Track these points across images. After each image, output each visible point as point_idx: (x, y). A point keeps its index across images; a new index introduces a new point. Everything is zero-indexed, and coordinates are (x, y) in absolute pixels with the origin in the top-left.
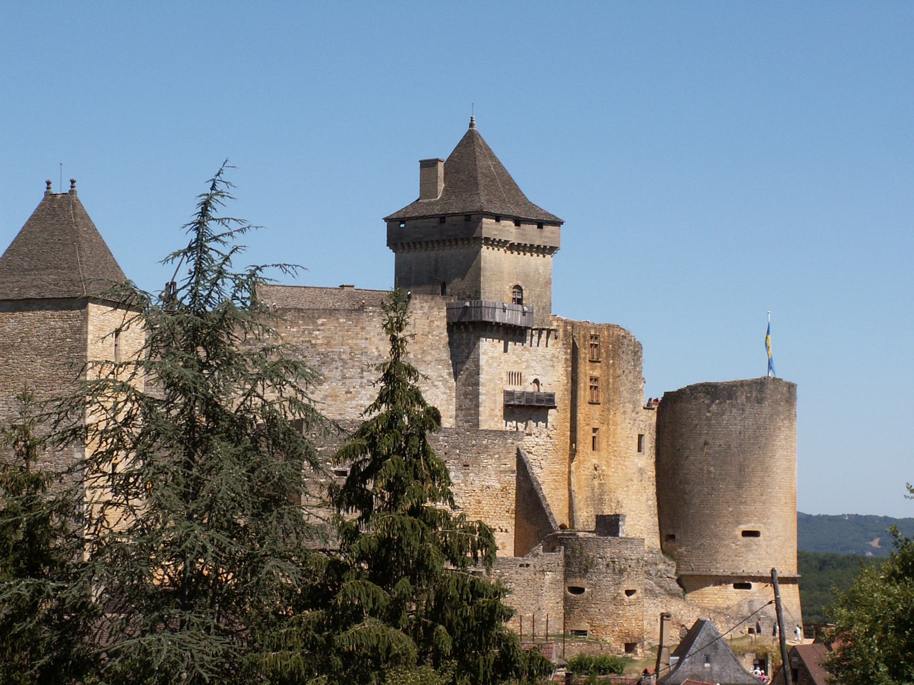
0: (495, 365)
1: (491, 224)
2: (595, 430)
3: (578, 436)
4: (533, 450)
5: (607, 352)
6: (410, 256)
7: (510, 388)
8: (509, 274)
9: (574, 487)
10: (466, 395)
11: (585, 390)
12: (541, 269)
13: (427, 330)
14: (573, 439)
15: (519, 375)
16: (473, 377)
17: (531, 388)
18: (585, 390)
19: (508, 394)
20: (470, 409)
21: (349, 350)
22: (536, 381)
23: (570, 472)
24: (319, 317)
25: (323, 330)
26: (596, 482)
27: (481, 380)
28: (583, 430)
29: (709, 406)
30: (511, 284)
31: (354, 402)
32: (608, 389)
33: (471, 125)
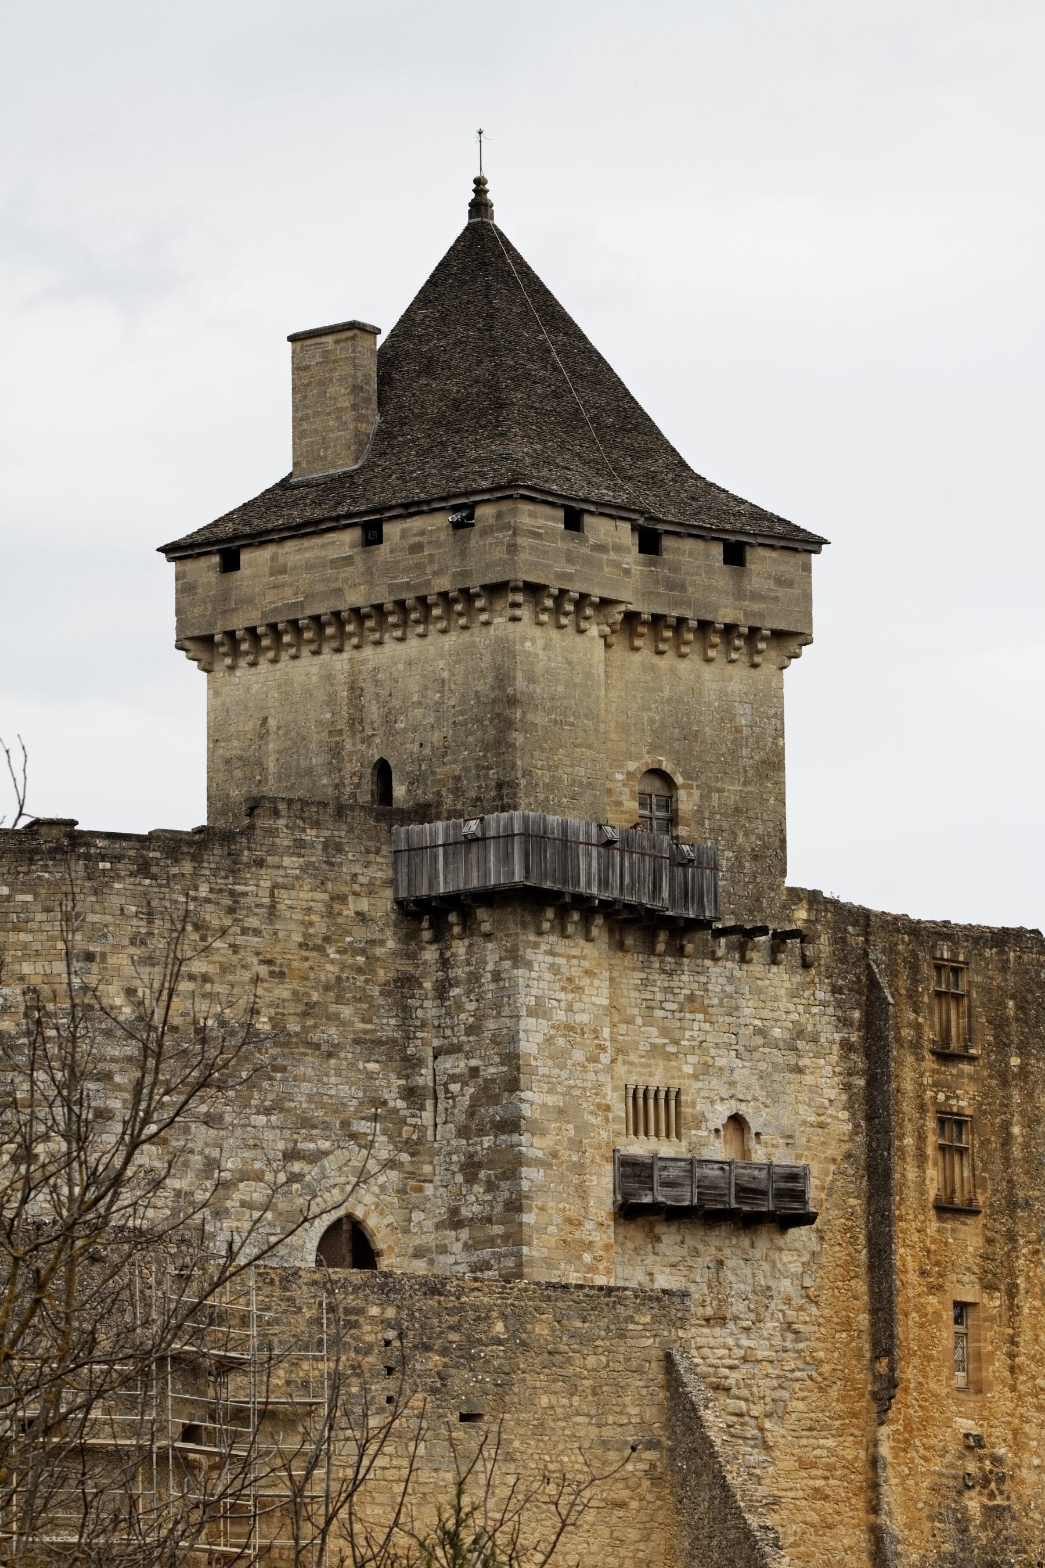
0: (578, 1056)
1: (551, 533)
2: (962, 1309)
3: (900, 1331)
4: (733, 1378)
5: (999, 1025)
6: (259, 679)
7: (639, 1148)
8: (624, 728)
9: (895, 1522)
10: (471, 1168)
11: (921, 1159)
12: (743, 716)
13: (320, 927)
14: (883, 1342)
15: (673, 1097)
16: (495, 1100)
17: (719, 1150)
18: (921, 1159)
19: (633, 1171)
20: (489, 1220)
22: (737, 1121)
23: (874, 1462)
26: (973, 1503)
27: (526, 1110)
28: (921, 1309)
30: (632, 766)
32: (1007, 1160)
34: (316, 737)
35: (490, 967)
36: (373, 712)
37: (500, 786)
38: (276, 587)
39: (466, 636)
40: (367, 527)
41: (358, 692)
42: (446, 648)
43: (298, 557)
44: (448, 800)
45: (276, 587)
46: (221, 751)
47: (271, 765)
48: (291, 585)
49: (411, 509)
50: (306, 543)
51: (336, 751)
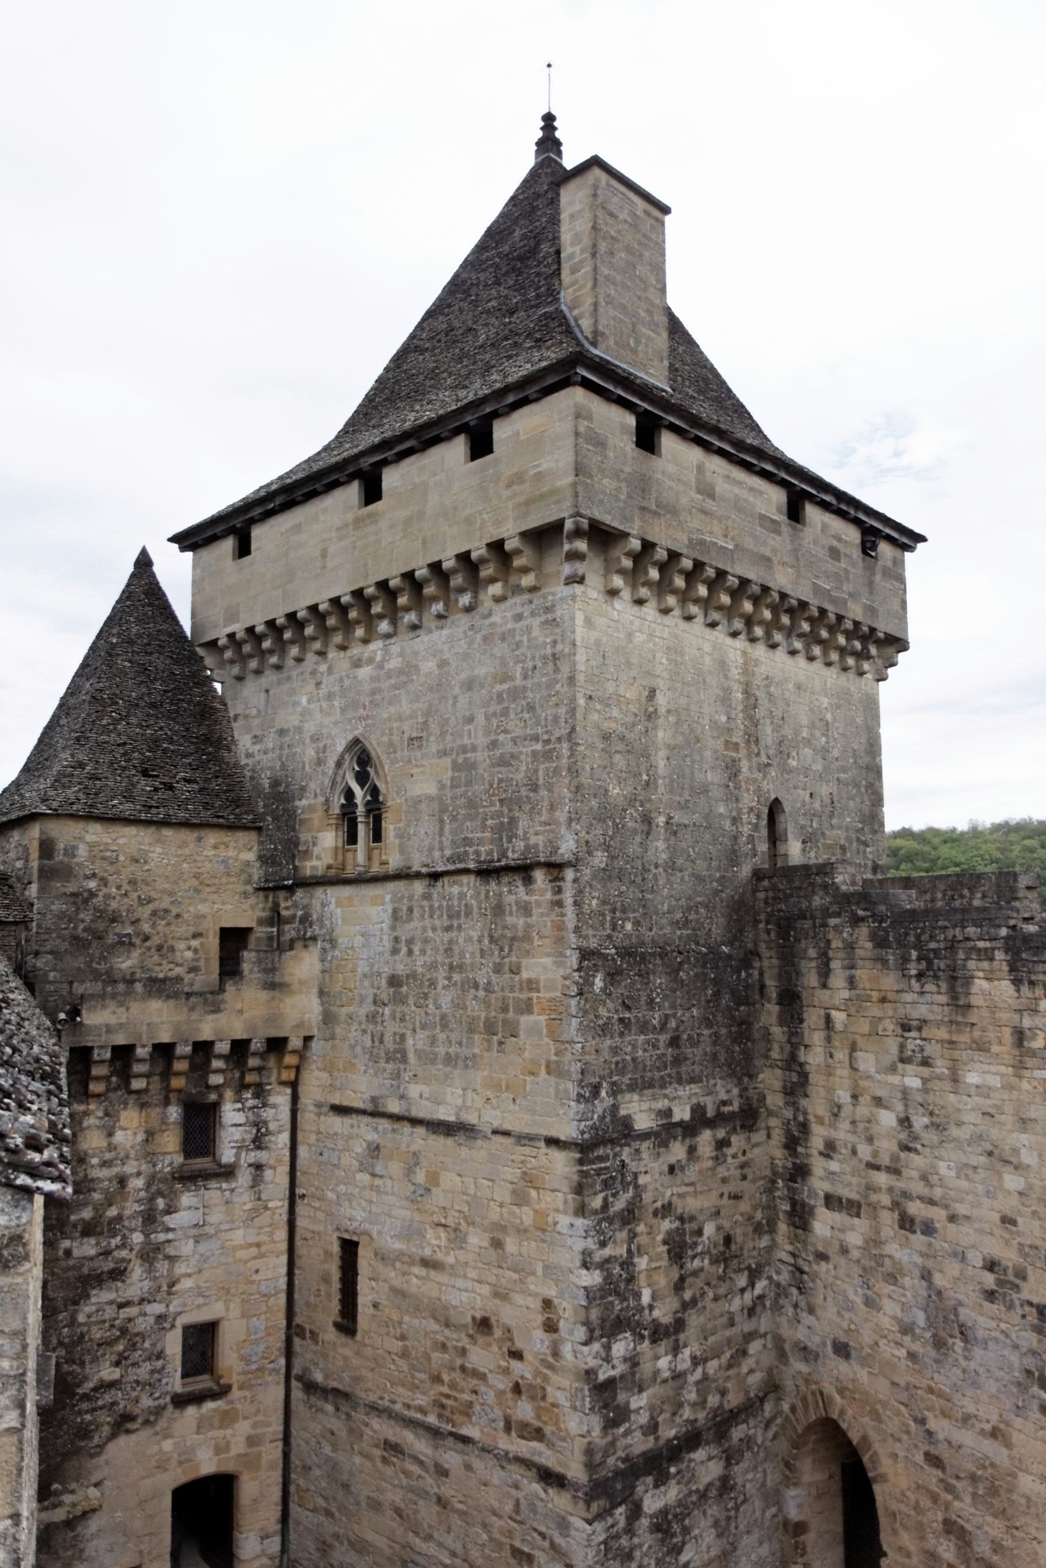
34: (711, 743)
36: (768, 734)
38: (703, 512)
39: (844, 677)
41: (752, 701)
42: (829, 684)
43: (727, 486)
45: (703, 512)
46: (595, 717)
47: (662, 763)
48: (720, 519)
51: (732, 770)
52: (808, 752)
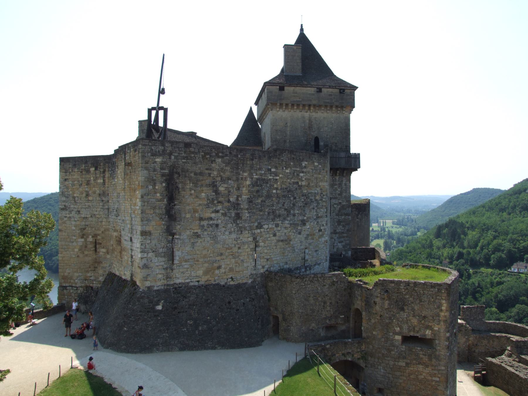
10: (339, 222)
20: (343, 233)
21: (320, 192)
24: (303, 160)
25: (306, 173)
29: (357, 215)
31: (323, 239)
33: (302, 30)
35: (344, 182)
37: (346, 146)
39: (338, 115)
40: (317, 88)
44: (334, 147)
49: (330, 87)
50: (302, 88)
52: (326, 128)
